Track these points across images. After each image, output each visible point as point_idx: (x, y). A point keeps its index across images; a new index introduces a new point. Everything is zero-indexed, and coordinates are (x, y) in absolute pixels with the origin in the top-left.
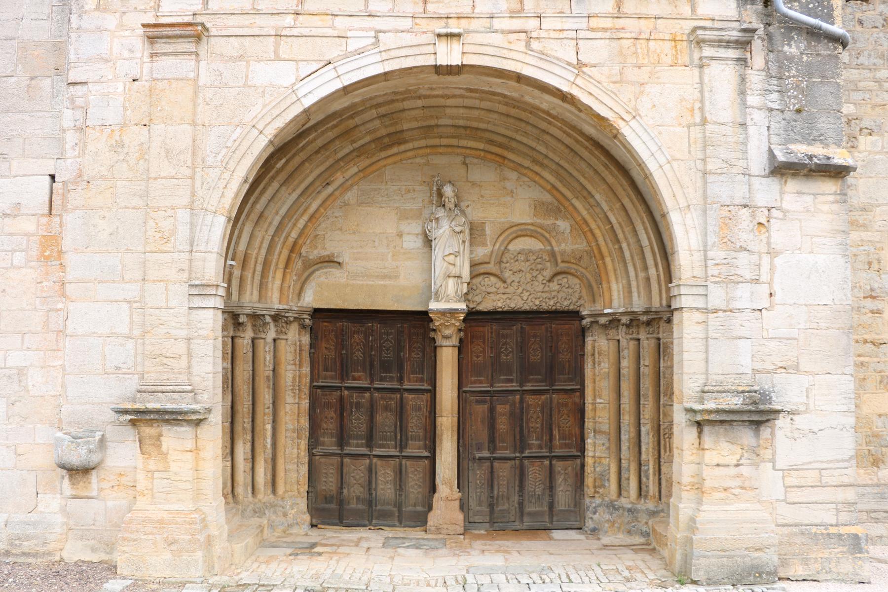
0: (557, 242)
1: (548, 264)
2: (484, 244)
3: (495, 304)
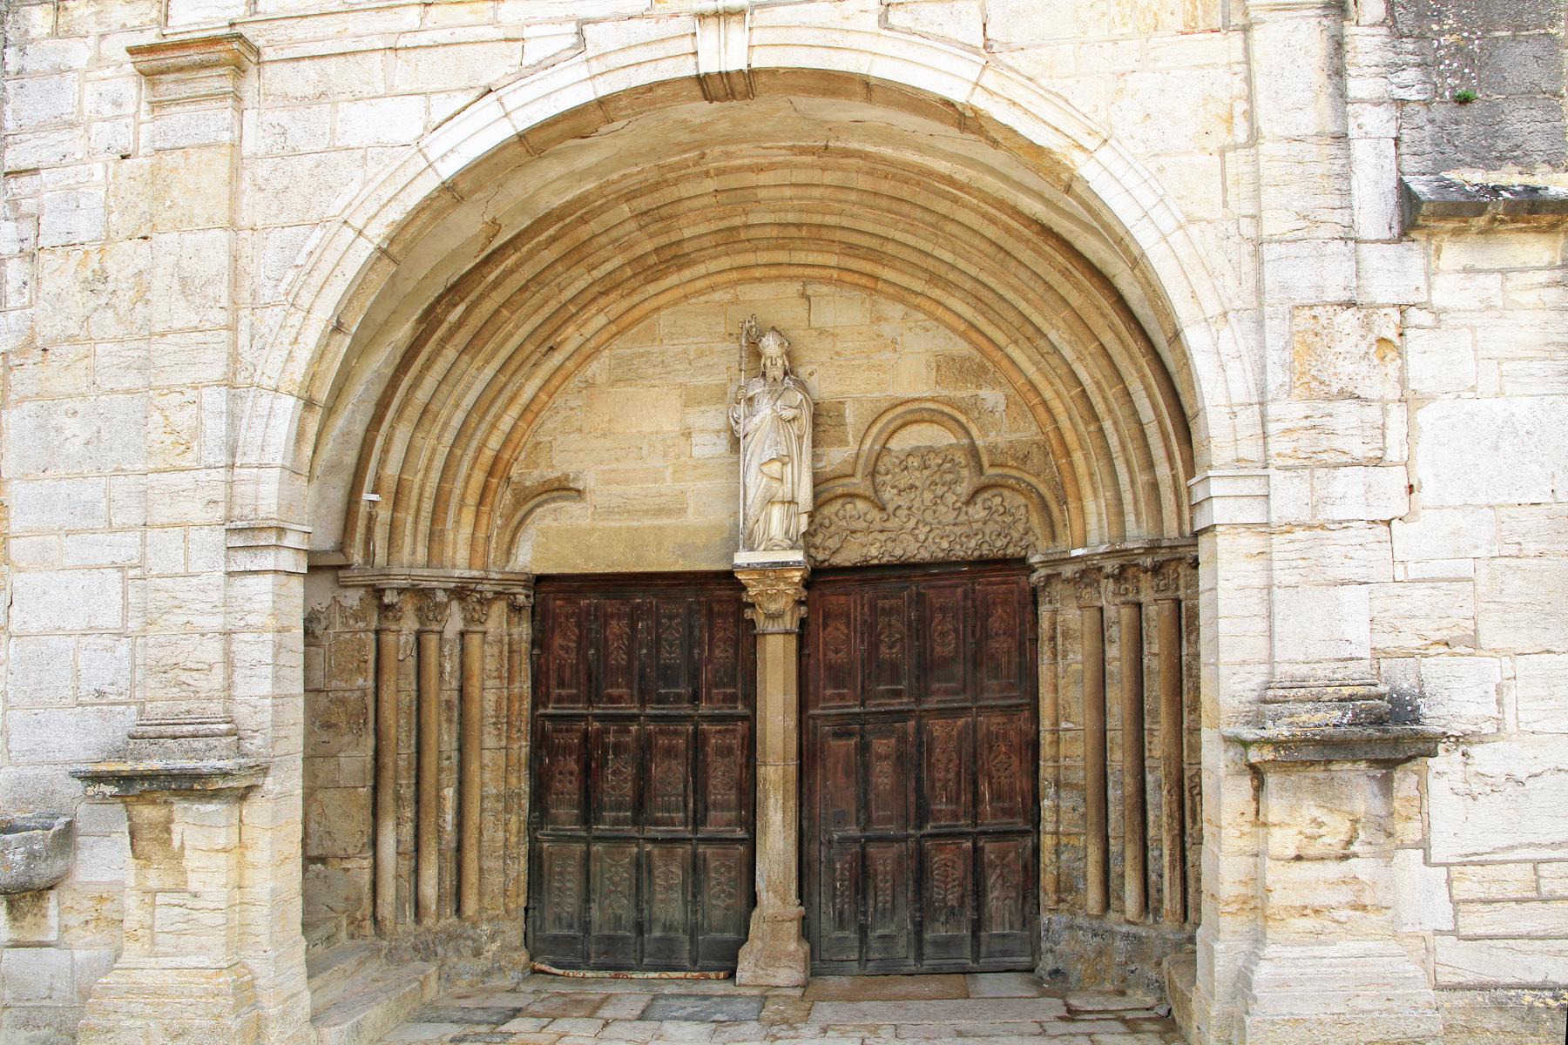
2: (843, 442)
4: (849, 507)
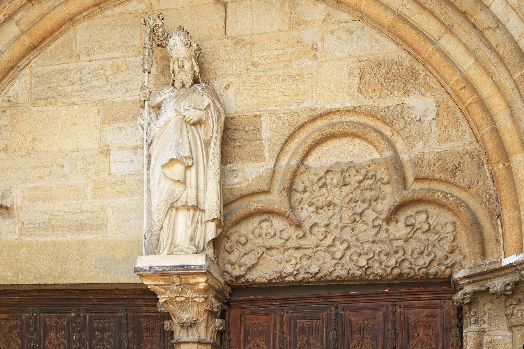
0: (406, 140)
1: (387, 189)
2: (258, 157)
3: (280, 267)
4: (265, 224)
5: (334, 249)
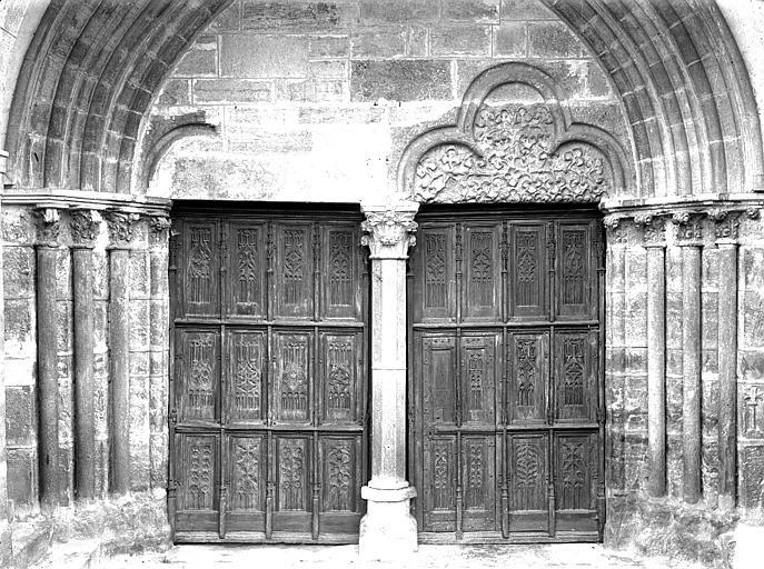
5: (509, 177)
